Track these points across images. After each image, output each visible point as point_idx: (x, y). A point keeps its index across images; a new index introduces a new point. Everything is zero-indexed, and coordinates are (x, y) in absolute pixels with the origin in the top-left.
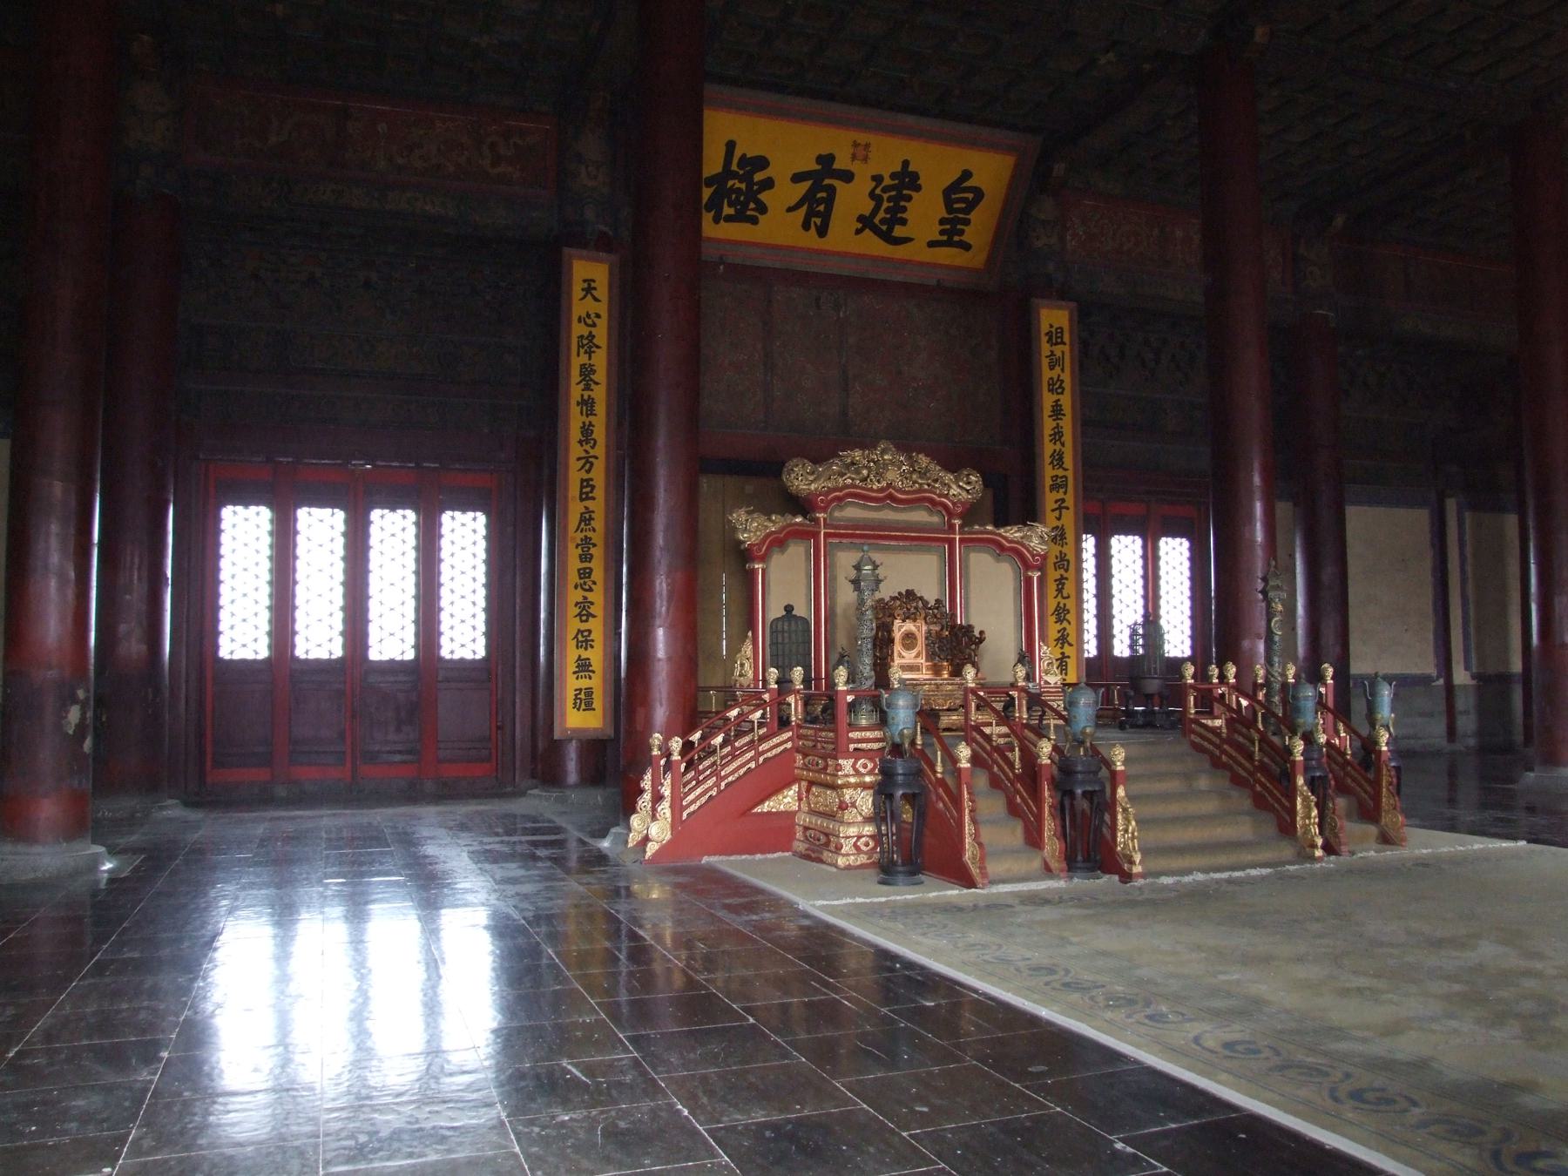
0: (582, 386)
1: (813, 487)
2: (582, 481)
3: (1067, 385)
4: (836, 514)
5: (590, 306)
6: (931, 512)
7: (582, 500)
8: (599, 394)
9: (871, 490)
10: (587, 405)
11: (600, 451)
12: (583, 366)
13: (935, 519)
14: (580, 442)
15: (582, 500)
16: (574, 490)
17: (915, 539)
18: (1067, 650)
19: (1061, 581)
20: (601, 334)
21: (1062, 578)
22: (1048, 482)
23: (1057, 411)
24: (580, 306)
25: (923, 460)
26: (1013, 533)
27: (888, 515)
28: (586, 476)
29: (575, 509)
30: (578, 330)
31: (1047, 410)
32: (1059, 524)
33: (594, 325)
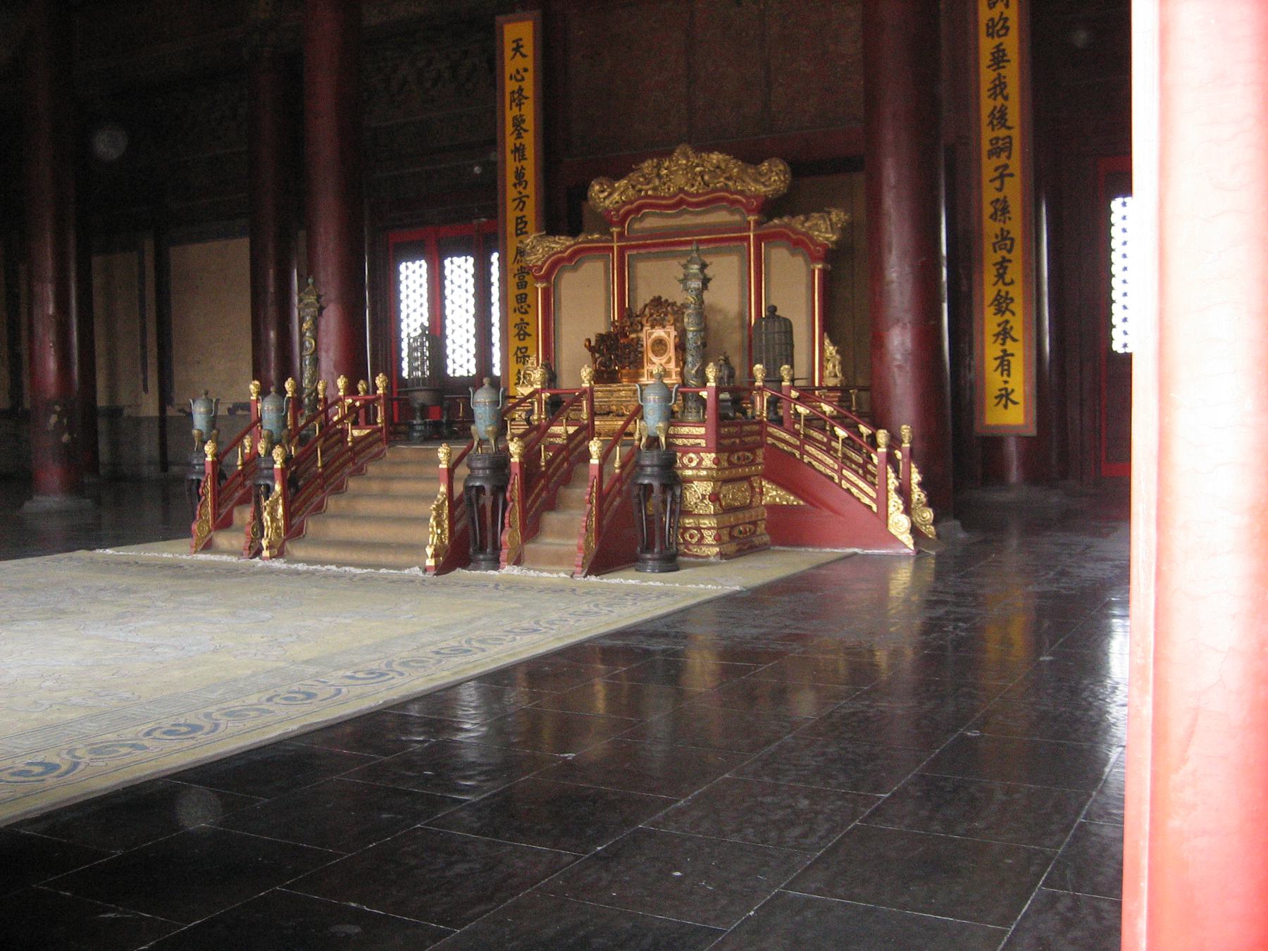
1: (607, 202)
3: (1013, 23)
4: (637, 226)
5: (520, 62)
6: (732, 213)
7: (517, 235)
8: (529, 140)
9: (664, 198)
10: (519, 151)
11: (530, 190)
12: (515, 118)
13: (737, 218)
14: (515, 185)
15: (517, 235)
16: (511, 228)
17: (722, 239)
18: (1010, 346)
19: (1002, 265)
20: (529, 86)
21: (1004, 260)
22: (986, 146)
23: (999, 58)
24: (511, 64)
25: (715, 157)
26: (799, 223)
27: (688, 220)
28: (520, 214)
29: (512, 243)
30: (511, 86)
31: (985, 58)
32: (1000, 195)
33: (523, 79)
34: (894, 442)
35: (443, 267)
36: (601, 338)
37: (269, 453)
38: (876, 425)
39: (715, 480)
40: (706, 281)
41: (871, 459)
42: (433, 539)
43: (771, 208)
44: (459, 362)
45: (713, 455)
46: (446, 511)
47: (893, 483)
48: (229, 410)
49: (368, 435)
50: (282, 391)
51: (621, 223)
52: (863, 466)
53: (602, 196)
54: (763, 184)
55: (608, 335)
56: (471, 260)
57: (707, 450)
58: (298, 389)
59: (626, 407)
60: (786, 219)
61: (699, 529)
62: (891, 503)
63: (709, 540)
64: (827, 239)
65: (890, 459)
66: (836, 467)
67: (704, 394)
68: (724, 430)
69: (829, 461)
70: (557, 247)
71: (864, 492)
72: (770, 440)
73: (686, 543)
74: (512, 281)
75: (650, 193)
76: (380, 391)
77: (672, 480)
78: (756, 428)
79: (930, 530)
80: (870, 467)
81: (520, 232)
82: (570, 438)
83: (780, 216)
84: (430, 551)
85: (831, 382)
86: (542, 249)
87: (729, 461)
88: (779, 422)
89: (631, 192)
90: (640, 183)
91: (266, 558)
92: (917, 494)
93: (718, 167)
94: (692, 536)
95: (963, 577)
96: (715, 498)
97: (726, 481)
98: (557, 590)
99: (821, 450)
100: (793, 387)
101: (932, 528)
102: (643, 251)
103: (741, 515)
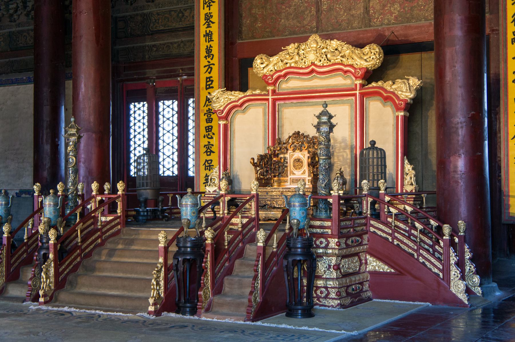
0: (206, 26)
1: (265, 70)
2: (207, 78)
7: (207, 89)
8: (215, 29)
9: (302, 68)
10: (209, 35)
11: (215, 61)
12: (206, 14)
15: (207, 89)
16: (203, 84)
25: (335, 43)
26: (388, 85)
28: (208, 75)
29: (203, 94)
34: (454, 232)
35: (157, 107)
36: (262, 158)
37: (47, 232)
38: (442, 219)
39: (338, 256)
40: (332, 127)
41: (439, 243)
42: (153, 293)
43: (371, 76)
44: (168, 166)
45: (337, 240)
46: (162, 274)
47: (453, 259)
48: (16, 193)
49: (111, 221)
50: (56, 191)
51: (274, 84)
52: (432, 247)
53: (263, 66)
54: (366, 60)
55: (266, 155)
56: (176, 103)
57: (332, 236)
58: (66, 190)
59: (277, 202)
60: (380, 83)
61: (326, 288)
62: (452, 273)
63: (333, 295)
64: (407, 96)
65: (452, 243)
66: (416, 248)
67: (331, 200)
68: (343, 224)
69: (411, 244)
70: (233, 98)
71: (435, 266)
72: (372, 229)
73: (318, 298)
74: (203, 118)
75: (293, 65)
76: (120, 193)
77: (311, 258)
78: (363, 221)
79: (478, 291)
80: (437, 247)
81: (209, 87)
82: (244, 226)
83: (377, 82)
84: (151, 301)
85: (409, 188)
86: (222, 98)
87: (346, 243)
88: (376, 216)
89: (281, 64)
90: (286, 59)
91: (41, 304)
92: (469, 267)
93: (336, 50)
94: (321, 292)
95: (502, 327)
96: (337, 267)
97: (344, 257)
98: (232, 329)
99: (403, 235)
100: (386, 194)
101: (479, 288)
102: (287, 102)
103: (353, 279)
